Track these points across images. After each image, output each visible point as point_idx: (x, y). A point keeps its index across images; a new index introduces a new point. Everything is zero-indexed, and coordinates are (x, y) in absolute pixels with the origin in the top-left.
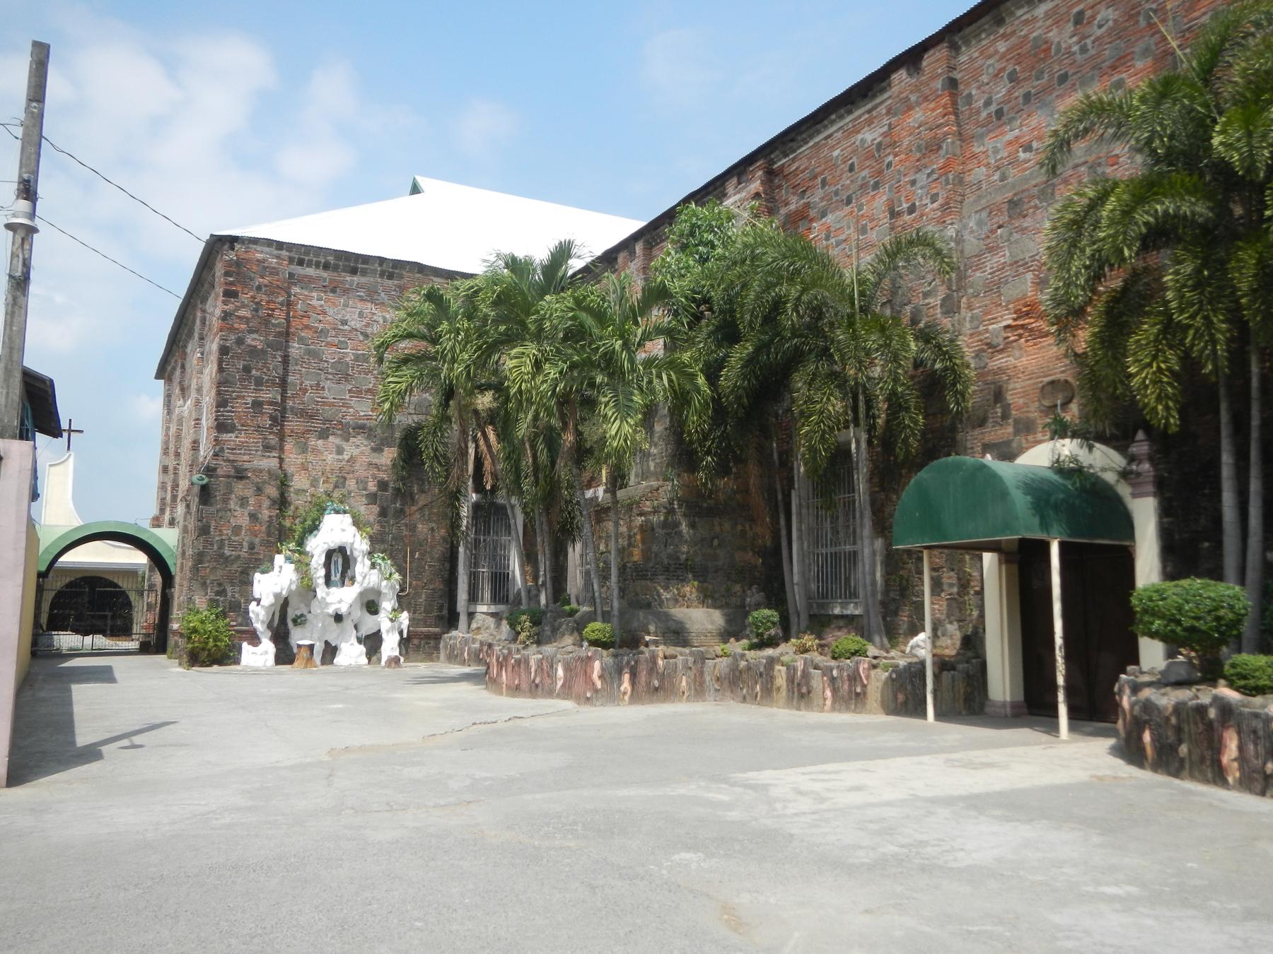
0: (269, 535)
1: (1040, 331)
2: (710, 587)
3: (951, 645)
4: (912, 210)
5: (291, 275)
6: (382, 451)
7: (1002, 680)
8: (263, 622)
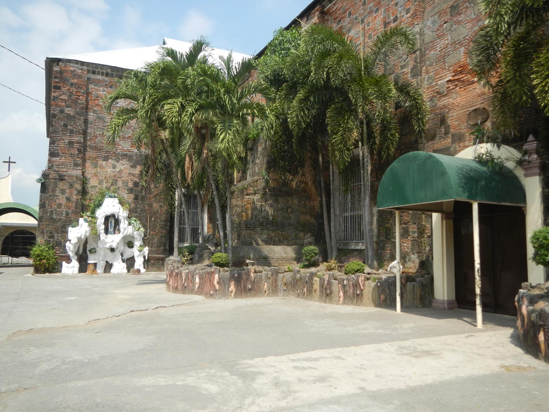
0: (76, 208)
1: (468, 81)
2: (286, 234)
3: (413, 266)
4: (395, 20)
5: (89, 79)
6: (136, 167)
7: (443, 288)
8: (72, 252)
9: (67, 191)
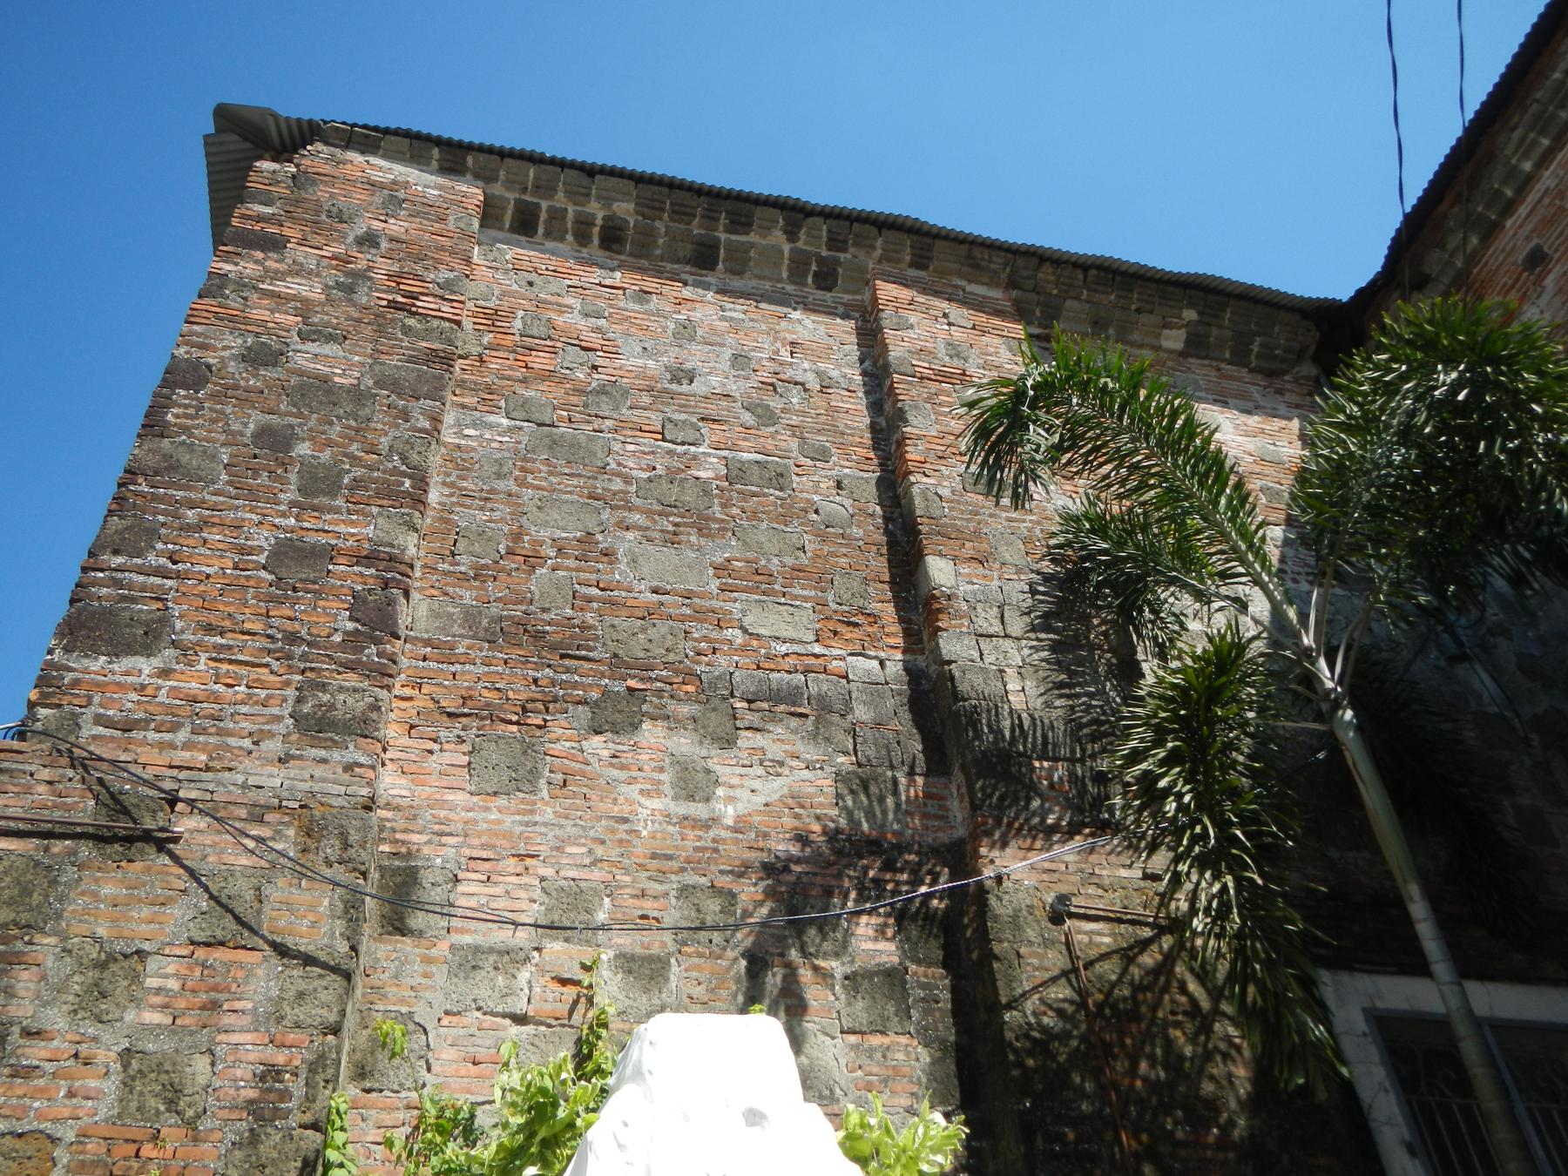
9: (163, 974)
